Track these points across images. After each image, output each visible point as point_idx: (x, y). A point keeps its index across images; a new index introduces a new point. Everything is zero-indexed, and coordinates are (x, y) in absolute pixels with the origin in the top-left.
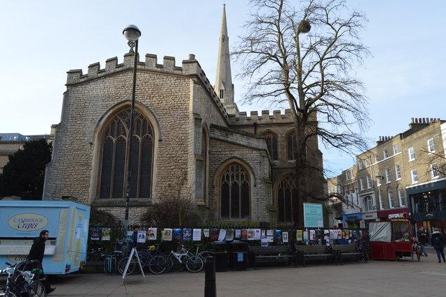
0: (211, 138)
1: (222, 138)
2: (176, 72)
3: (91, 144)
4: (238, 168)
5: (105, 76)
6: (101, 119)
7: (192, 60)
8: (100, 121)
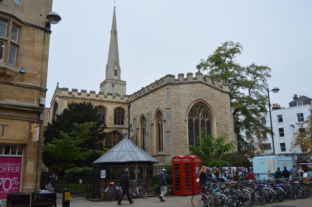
3: (186, 121)
5: (189, 83)
6: (189, 107)
8: (188, 108)
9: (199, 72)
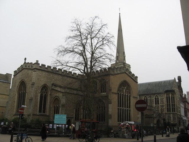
0: (52, 89)
1: (55, 89)
2: (32, 68)
4: (57, 100)
7: (37, 63)
9: (25, 62)
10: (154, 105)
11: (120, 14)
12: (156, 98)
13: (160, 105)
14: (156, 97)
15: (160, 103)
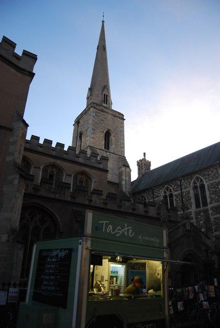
10: (193, 209)
11: (103, 21)
12: (195, 188)
13: (209, 206)
14: (195, 183)
15: (209, 200)
